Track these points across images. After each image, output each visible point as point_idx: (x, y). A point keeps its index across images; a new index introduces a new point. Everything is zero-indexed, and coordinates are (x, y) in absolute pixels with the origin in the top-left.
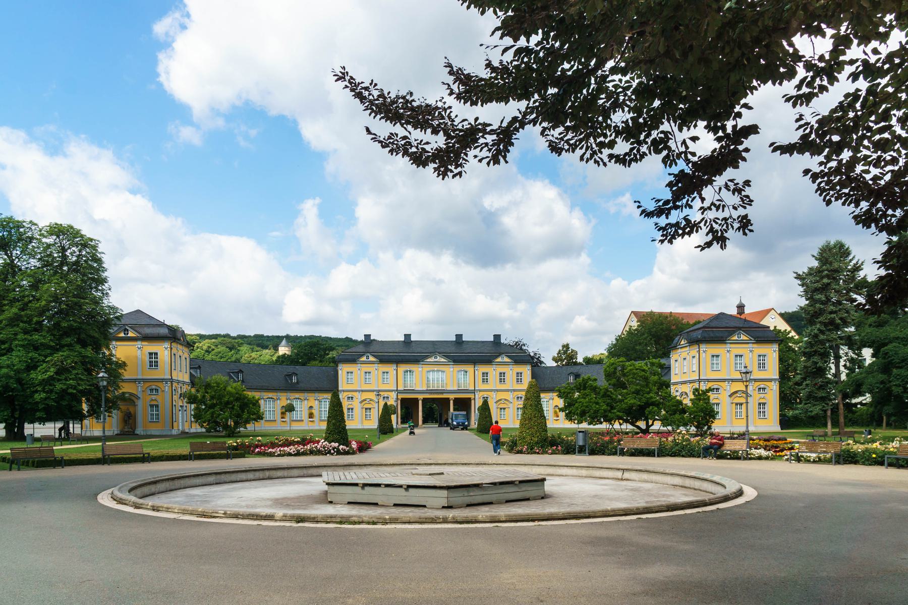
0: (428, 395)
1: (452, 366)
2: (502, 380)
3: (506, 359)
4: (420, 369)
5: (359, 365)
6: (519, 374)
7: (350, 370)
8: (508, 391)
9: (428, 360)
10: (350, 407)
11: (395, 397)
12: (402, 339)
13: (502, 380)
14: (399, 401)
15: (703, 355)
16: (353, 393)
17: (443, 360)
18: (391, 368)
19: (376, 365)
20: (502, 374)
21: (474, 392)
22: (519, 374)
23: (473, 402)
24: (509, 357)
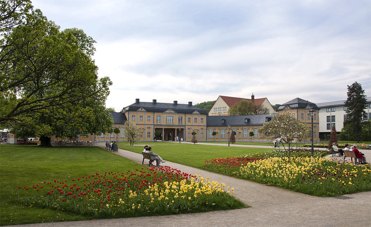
0: (166, 127)
1: (176, 114)
2: (196, 122)
3: (198, 113)
4: (164, 115)
5: (138, 112)
6: (202, 119)
7: (134, 114)
8: (198, 126)
9: (167, 112)
10: (149, 132)
11: (153, 128)
12: (152, 101)
13: (196, 122)
14: (155, 129)
15: (299, 113)
16: (150, 126)
17: (173, 112)
18: (151, 114)
19: (145, 113)
20: (196, 119)
21: (185, 126)
22: (202, 119)
23: (184, 130)
24: (198, 111)
